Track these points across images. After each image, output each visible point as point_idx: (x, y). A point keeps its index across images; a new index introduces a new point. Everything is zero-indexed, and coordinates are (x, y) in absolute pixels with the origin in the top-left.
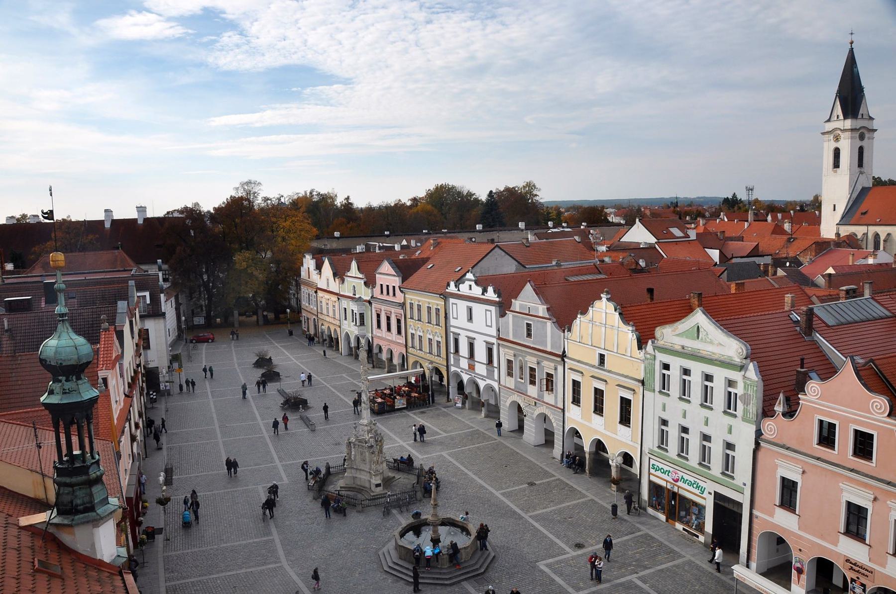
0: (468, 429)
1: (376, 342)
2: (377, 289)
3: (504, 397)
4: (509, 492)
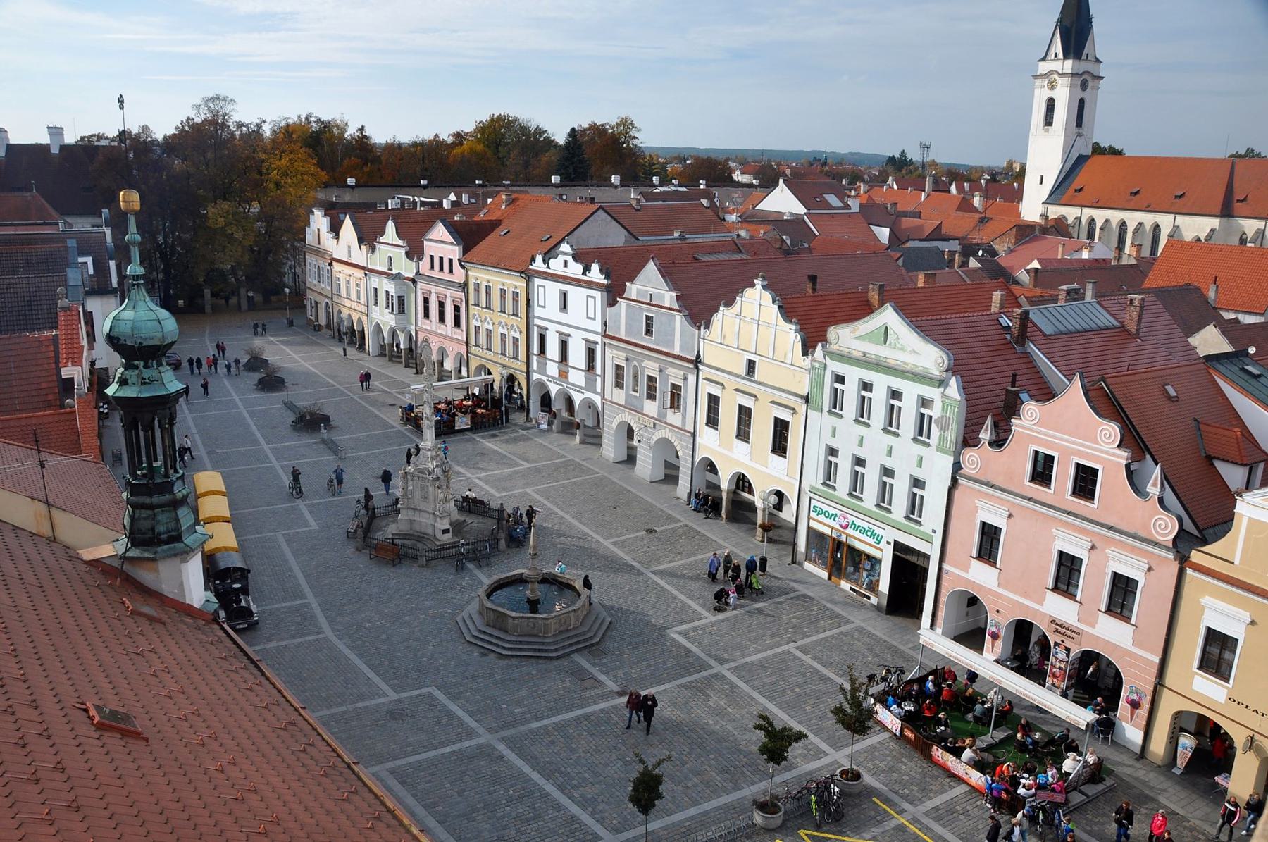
0: (558, 458)
1: (421, 337)
2: (425, 263)
3: (609, 416)
4: (624, 541)
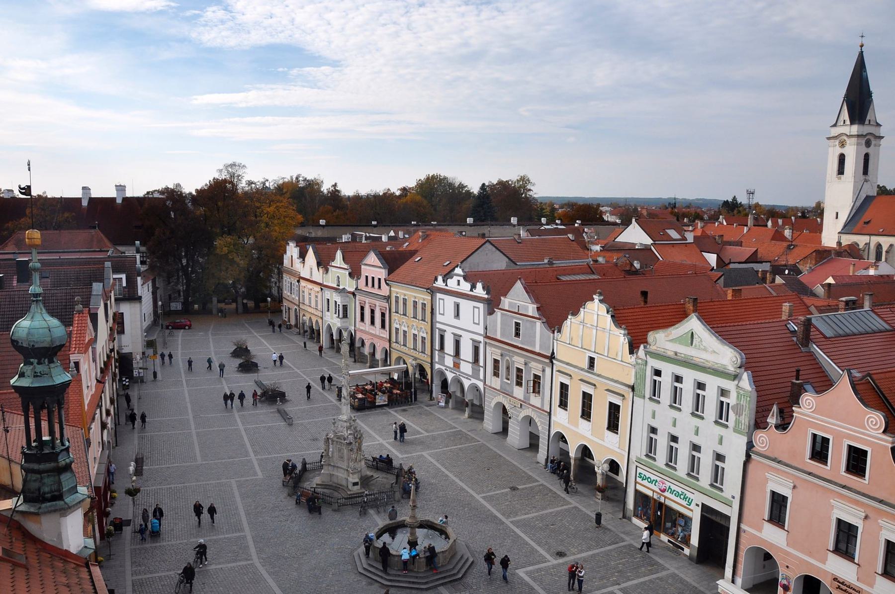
1: (358, 336)
2: (362, 281)
3: (489, 398)
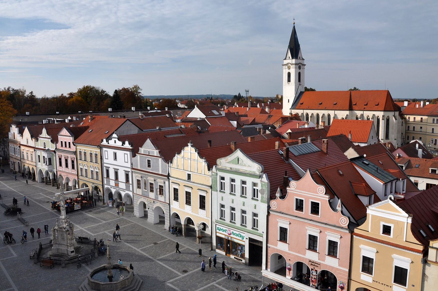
2: (59, 145)
